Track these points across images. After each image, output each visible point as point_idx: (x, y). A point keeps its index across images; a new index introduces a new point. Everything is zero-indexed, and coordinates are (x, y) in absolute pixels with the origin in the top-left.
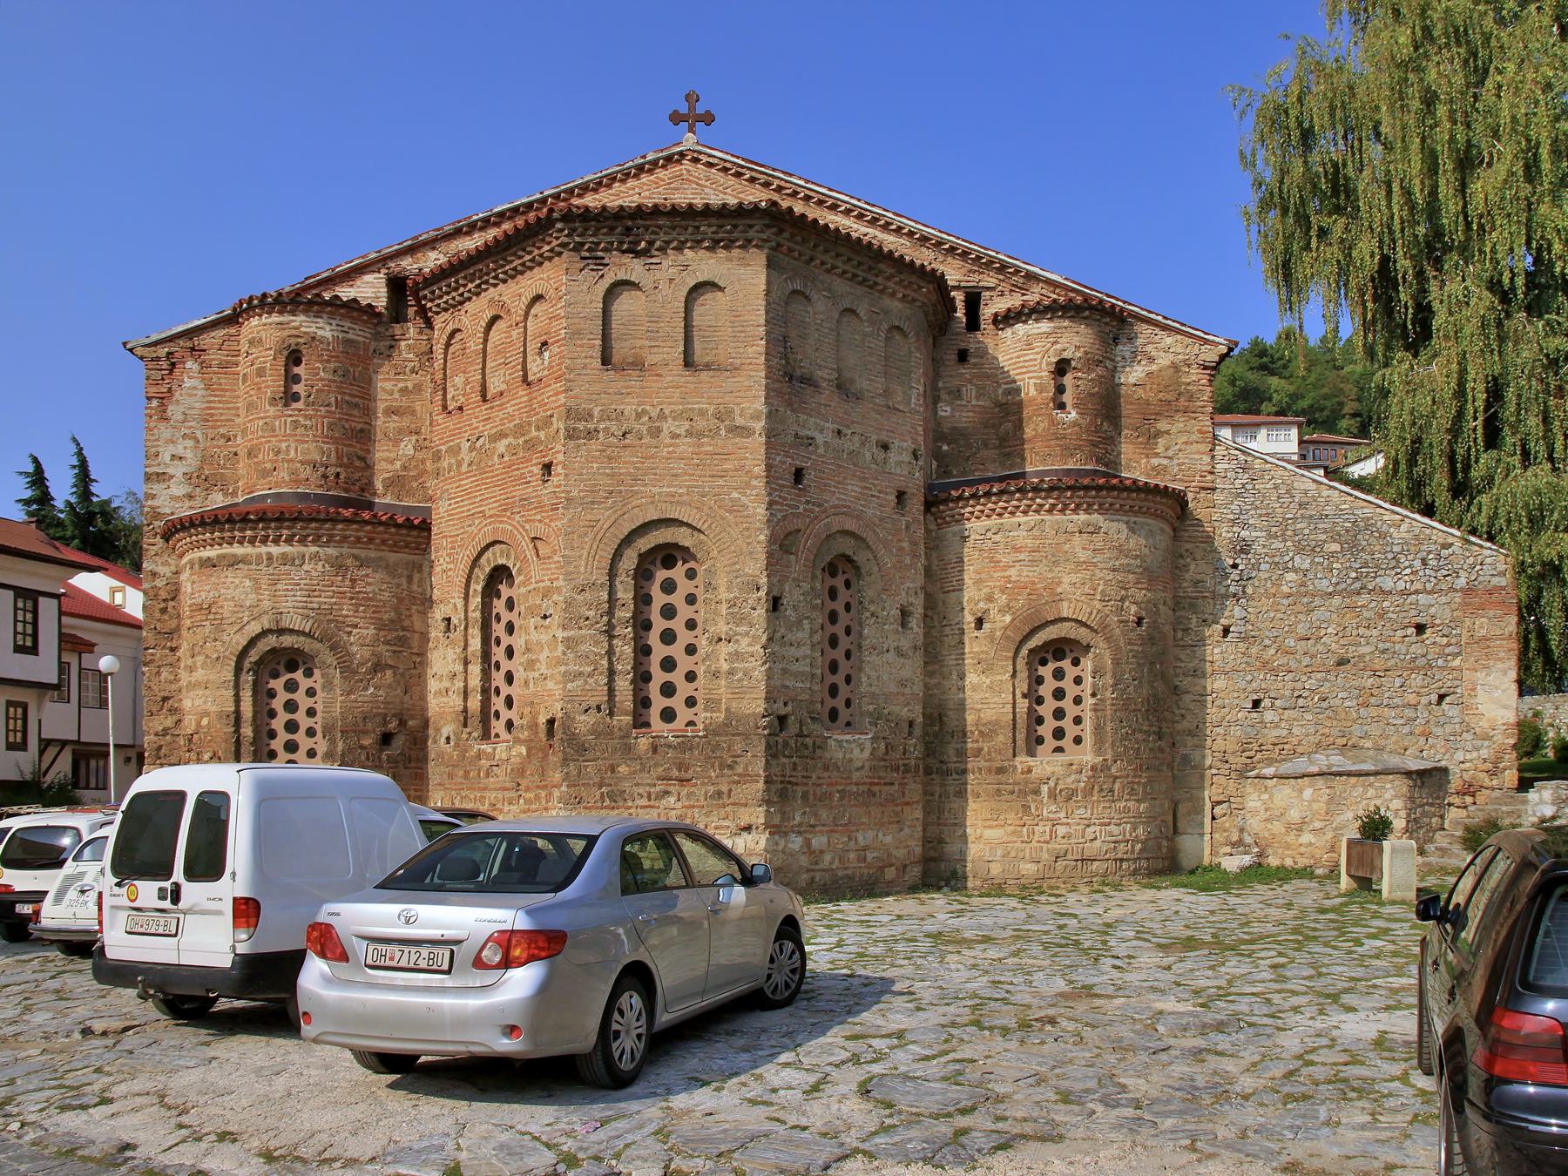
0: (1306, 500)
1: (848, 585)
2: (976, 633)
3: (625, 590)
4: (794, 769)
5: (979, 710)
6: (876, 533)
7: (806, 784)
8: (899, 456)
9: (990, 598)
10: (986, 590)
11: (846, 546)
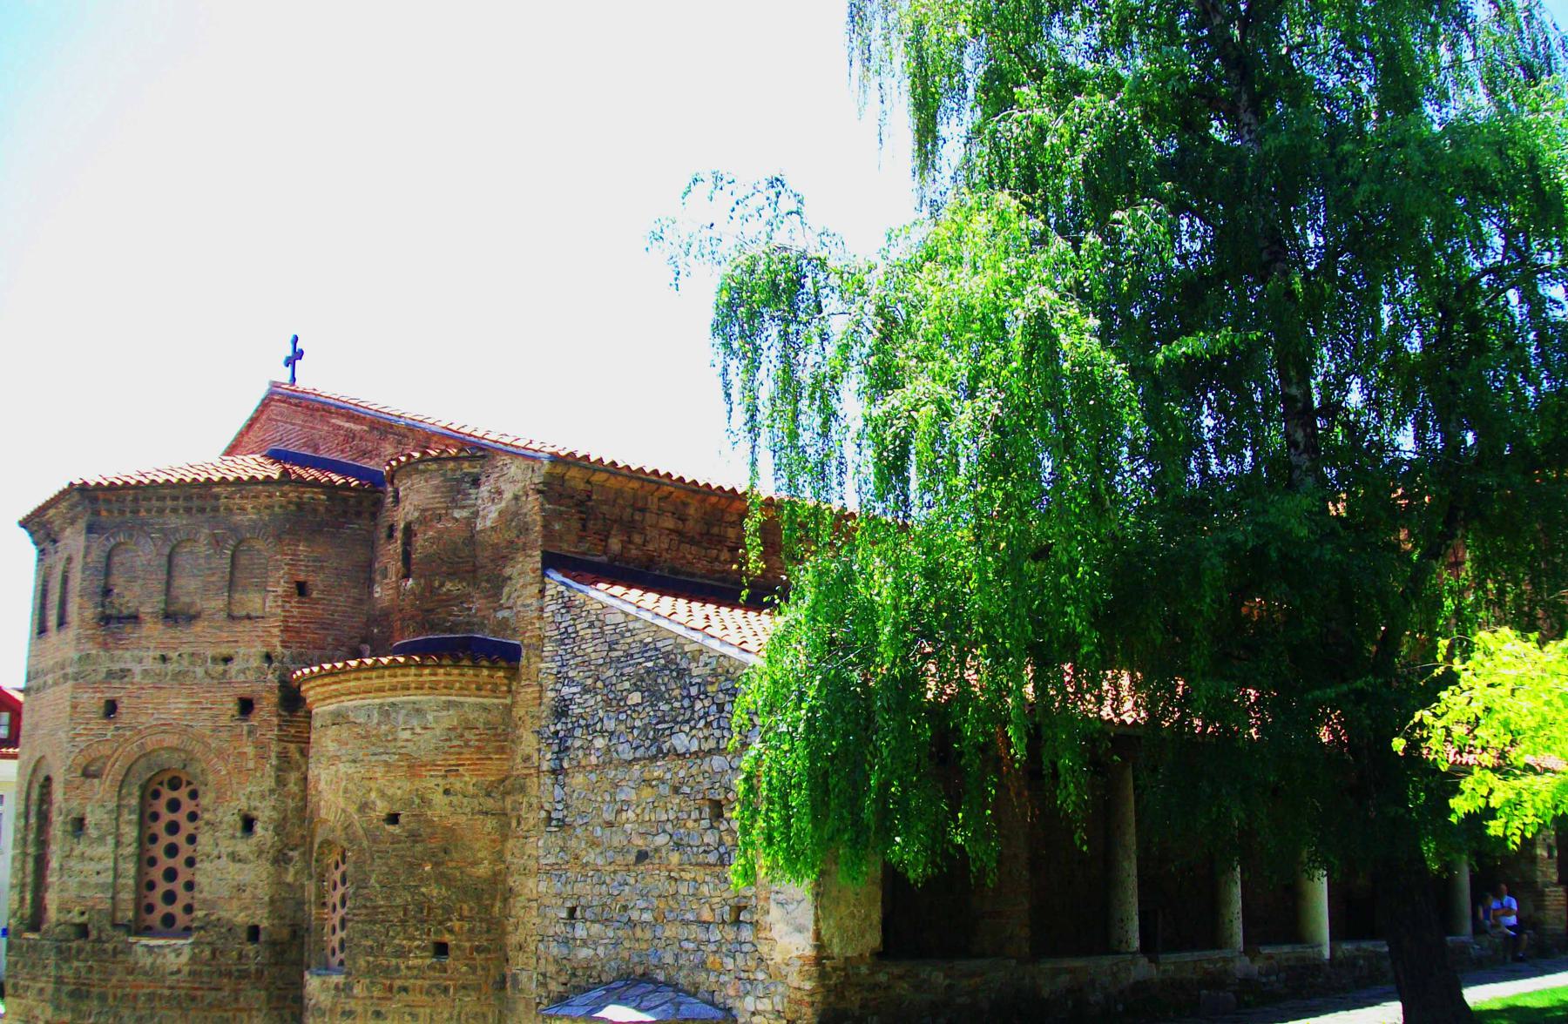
6: (207, 745)
11: (175, 761)
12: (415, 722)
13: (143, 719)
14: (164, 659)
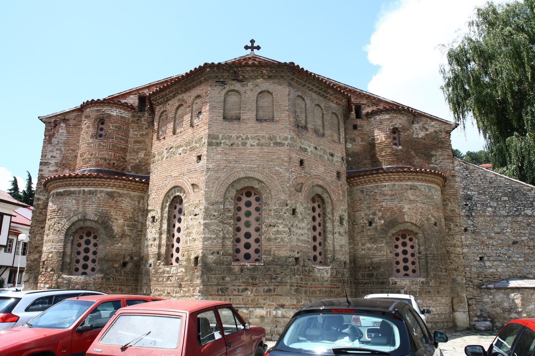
0: (492, 181)
1: (319, 206)
2: (369, 228)
3: (230, 205)
4: (302, 280)
5: (372, 258)
6: (330, 187)
7: (306, 287)
8: (337, 159)
9: (374, 214)
10: (373, 211)
11: (319, 191)
12: (436, 194)
13: (312, 171)
14: (316, 148)
